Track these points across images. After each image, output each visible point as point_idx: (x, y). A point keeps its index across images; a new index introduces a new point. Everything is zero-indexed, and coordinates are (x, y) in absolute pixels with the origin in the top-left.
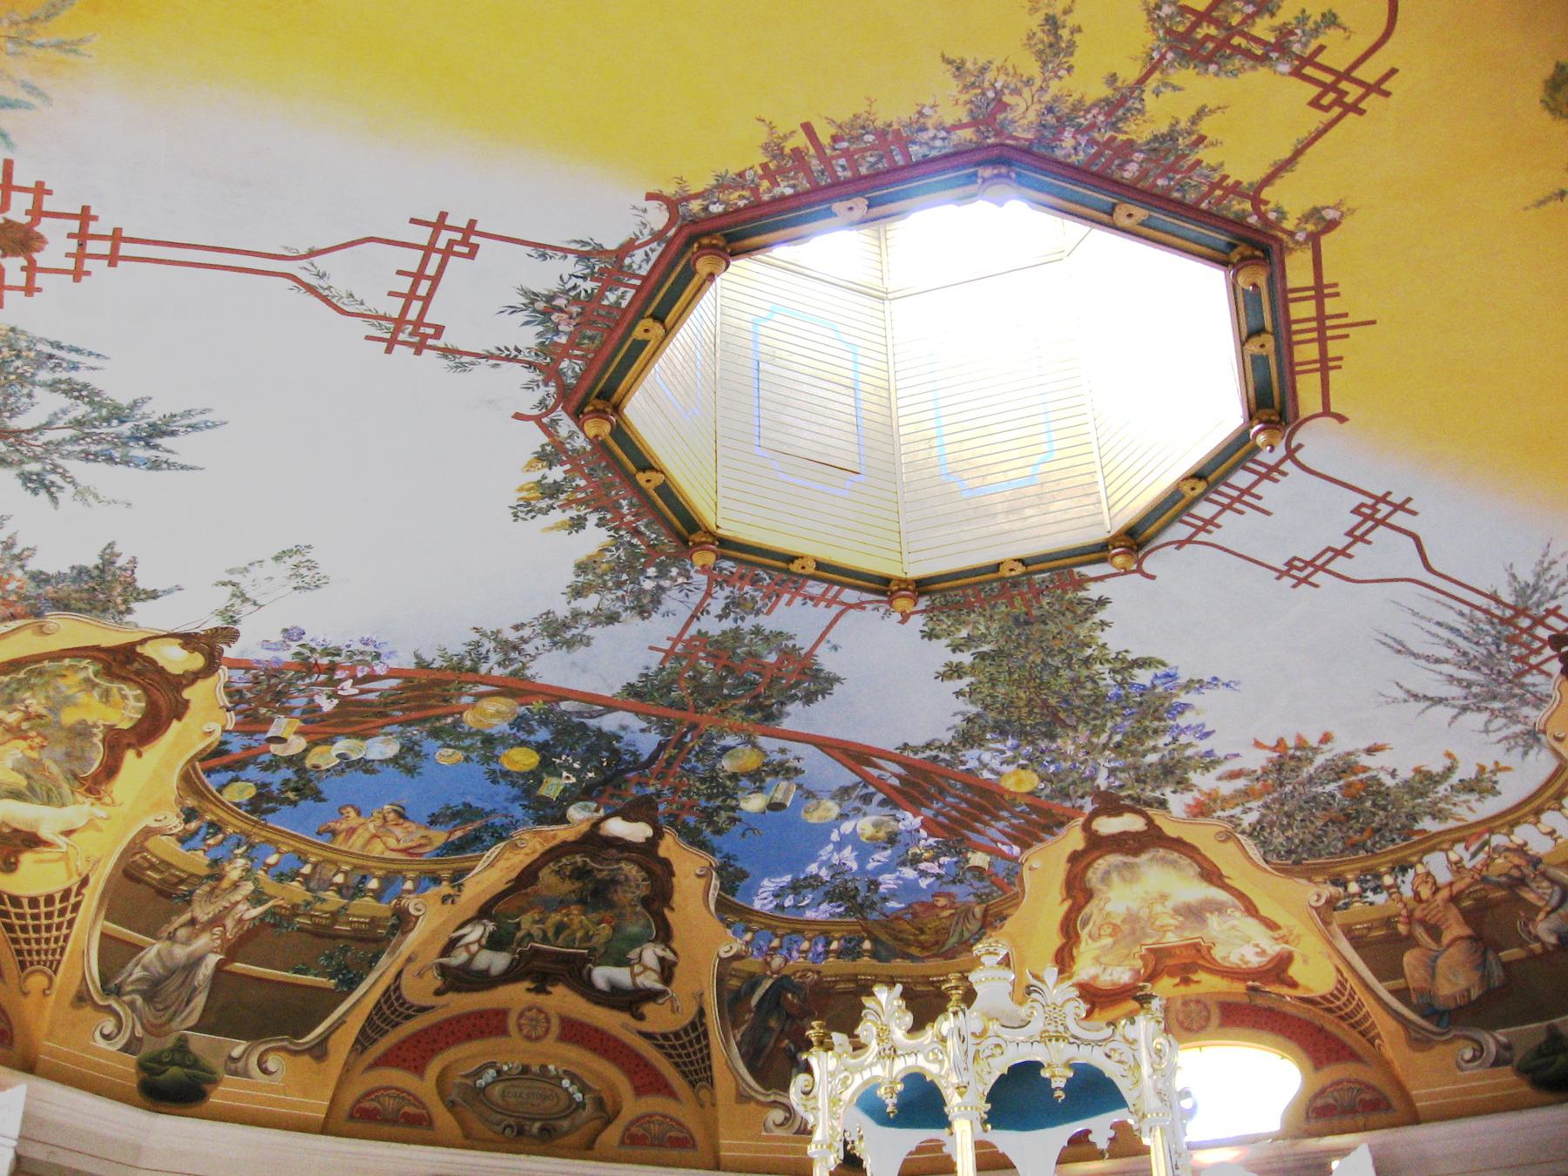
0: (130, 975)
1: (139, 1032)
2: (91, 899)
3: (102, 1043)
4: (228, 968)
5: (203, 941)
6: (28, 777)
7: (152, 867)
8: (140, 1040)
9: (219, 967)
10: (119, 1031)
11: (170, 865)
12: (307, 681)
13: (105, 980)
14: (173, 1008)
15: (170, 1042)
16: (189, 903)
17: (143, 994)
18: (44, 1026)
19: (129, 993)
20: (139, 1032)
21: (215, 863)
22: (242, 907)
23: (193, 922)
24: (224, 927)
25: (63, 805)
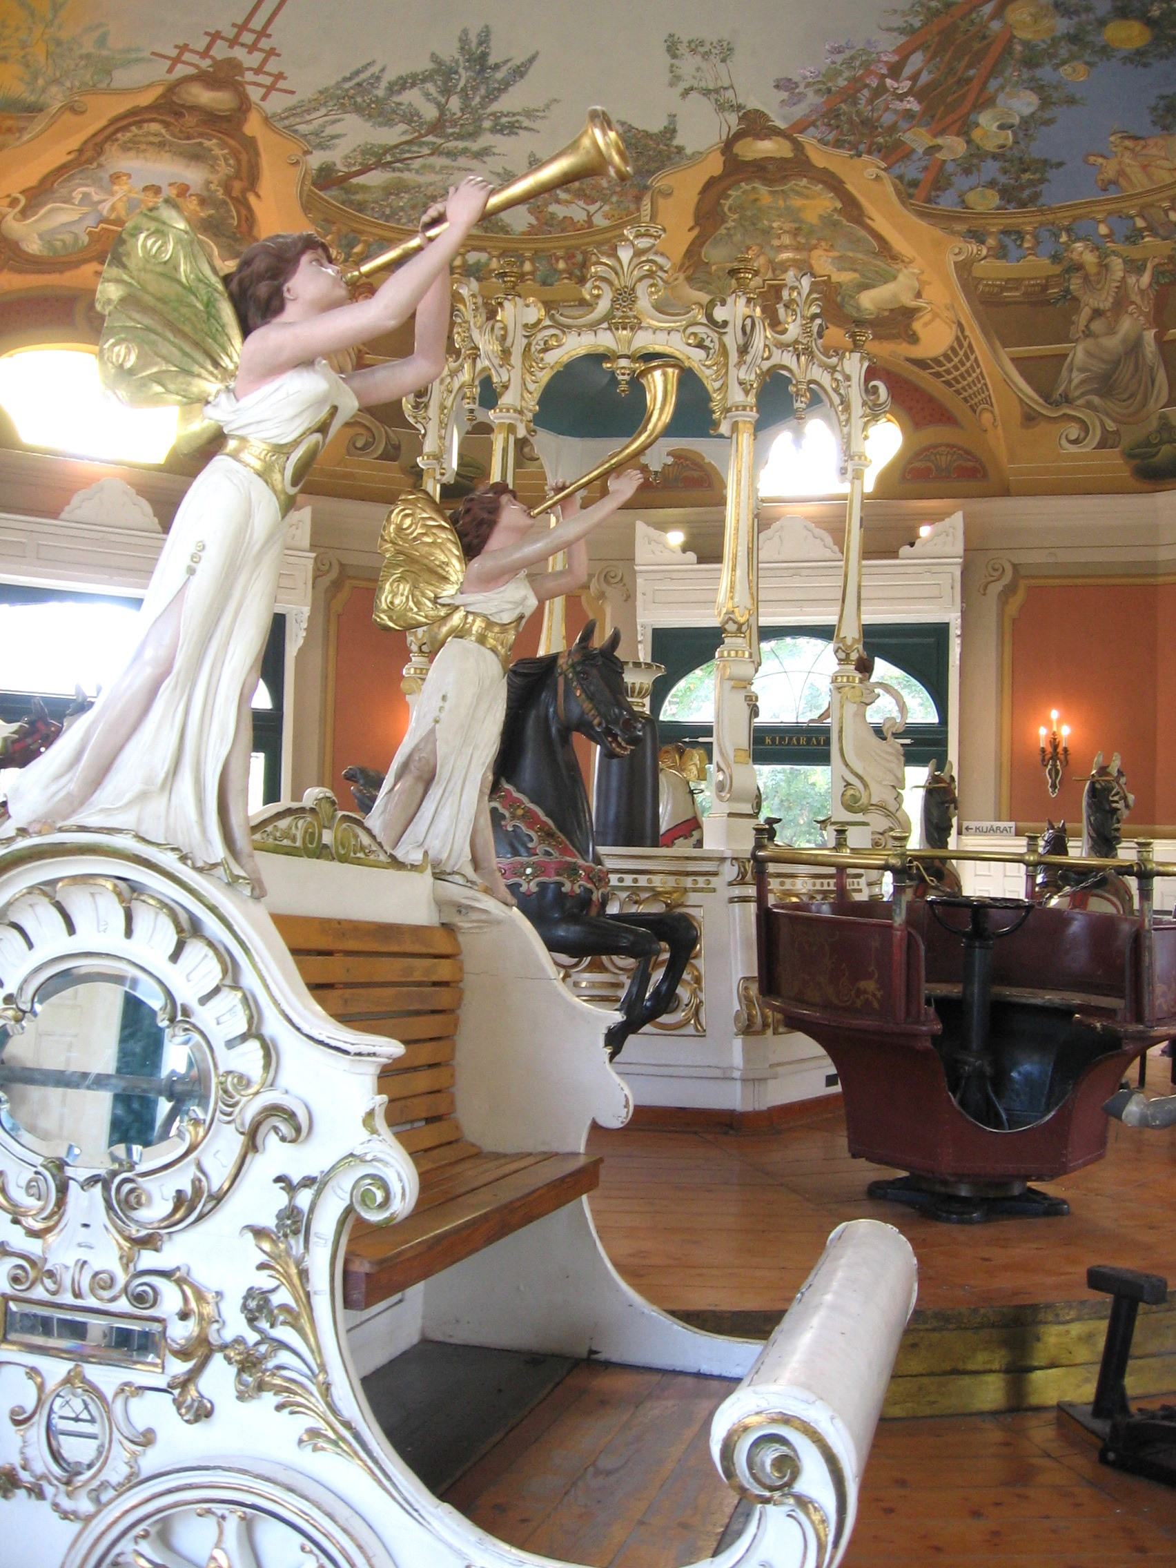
0: (1070, 381)
1: (1111, 426)
2: (975, 335)
3: (1073, 449)
4: (1166, 338)
5: (1126, 325)
6: (855, 271)
7: (1003, 289)
8: (1117, 432)
9: (1158, 338)
10: (1087, 433)
11: (1018, 281)
12: (863, 102)
13: (1047, 397)
14: (1139, 397)
15: (1154, 423)
16: (1075, 299)
17: (1097, 392)
18: (1002, 452)
19: (1078, 398)
20: (1111, 426)
21: (1056, 258)
22: (1132, 280)
23: (1097, 313)
24: (1133, 303)
25: (895, 278)
